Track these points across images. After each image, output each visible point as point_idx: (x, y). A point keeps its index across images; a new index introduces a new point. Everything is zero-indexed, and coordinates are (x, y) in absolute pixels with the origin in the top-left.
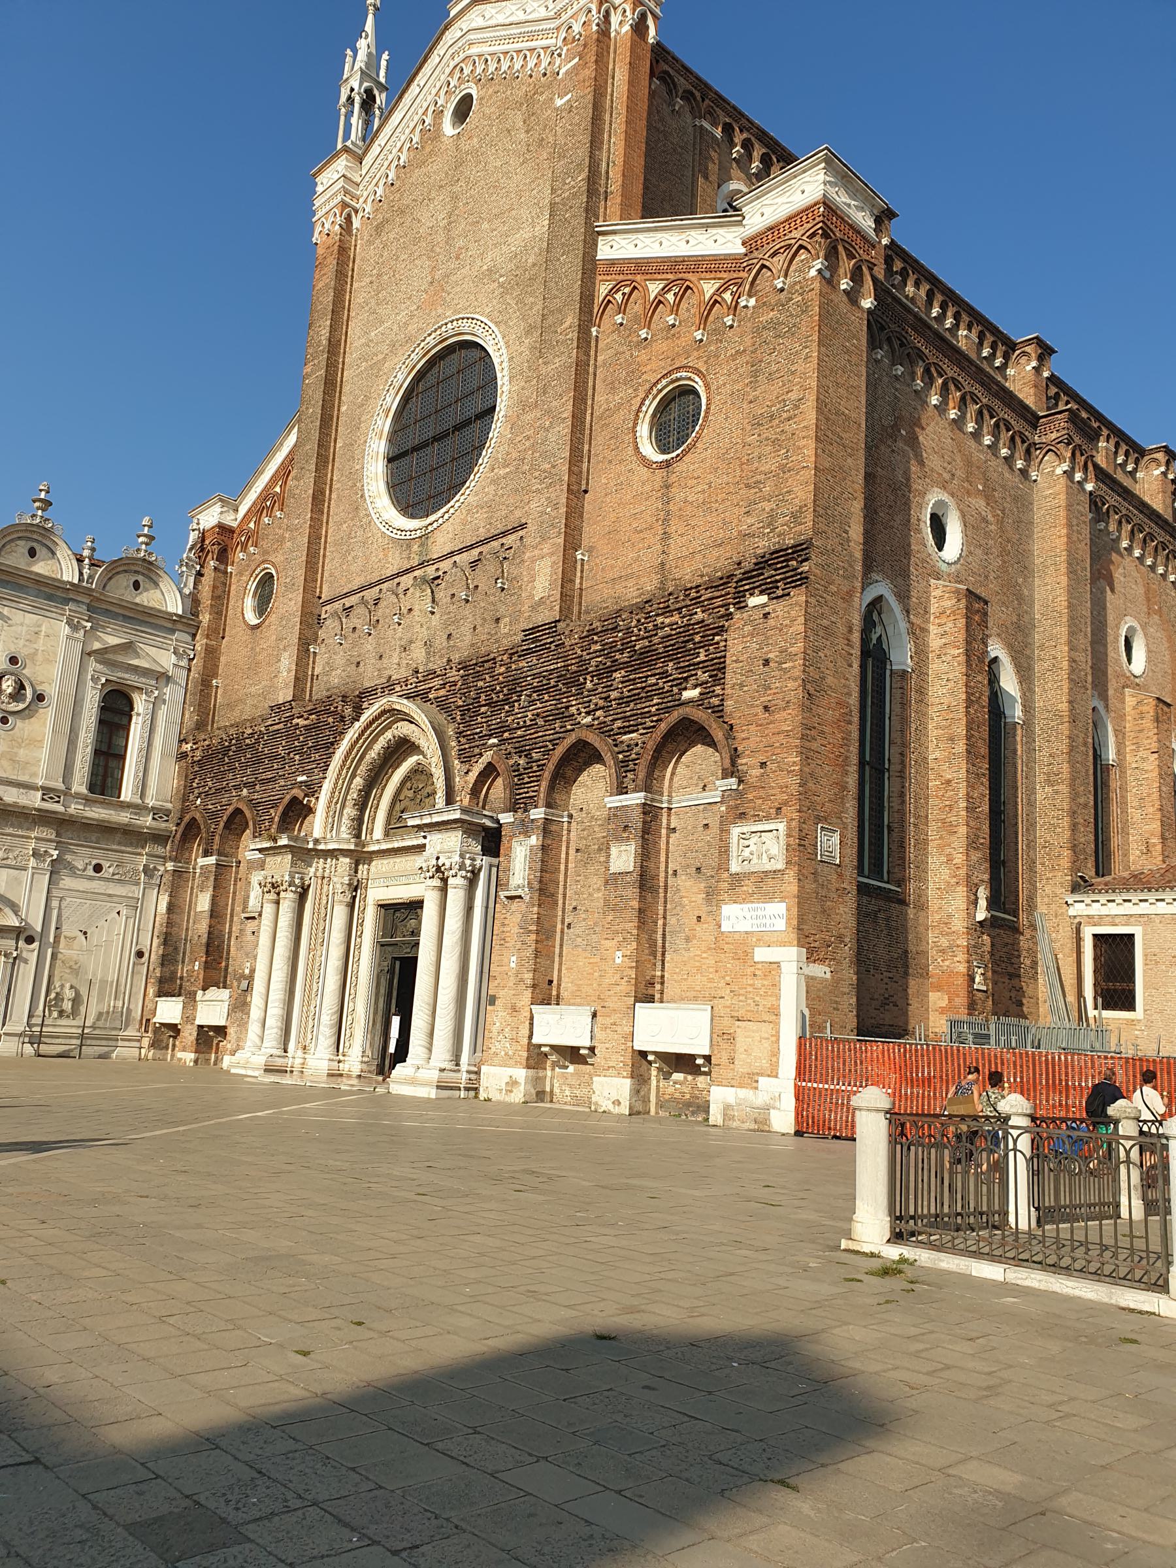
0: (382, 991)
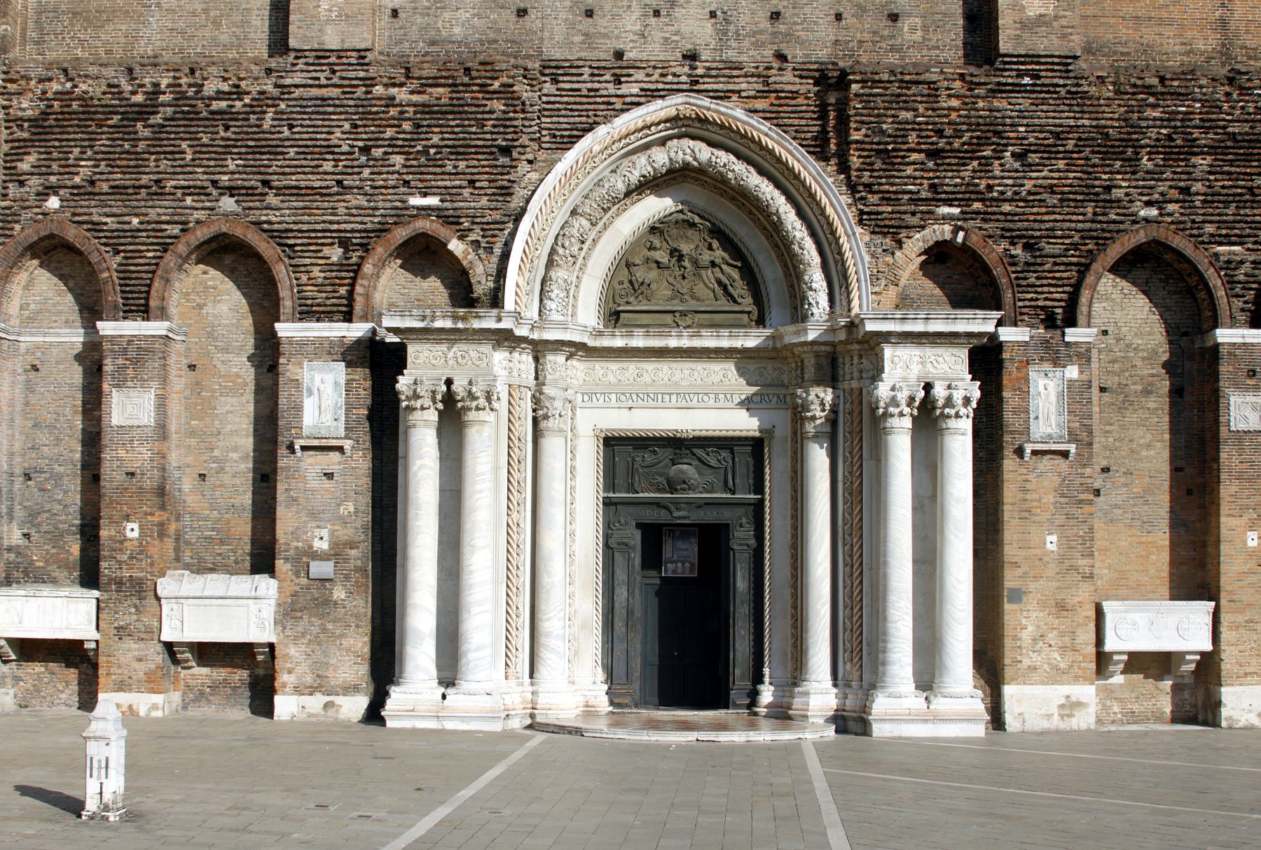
0: (621, 575)
